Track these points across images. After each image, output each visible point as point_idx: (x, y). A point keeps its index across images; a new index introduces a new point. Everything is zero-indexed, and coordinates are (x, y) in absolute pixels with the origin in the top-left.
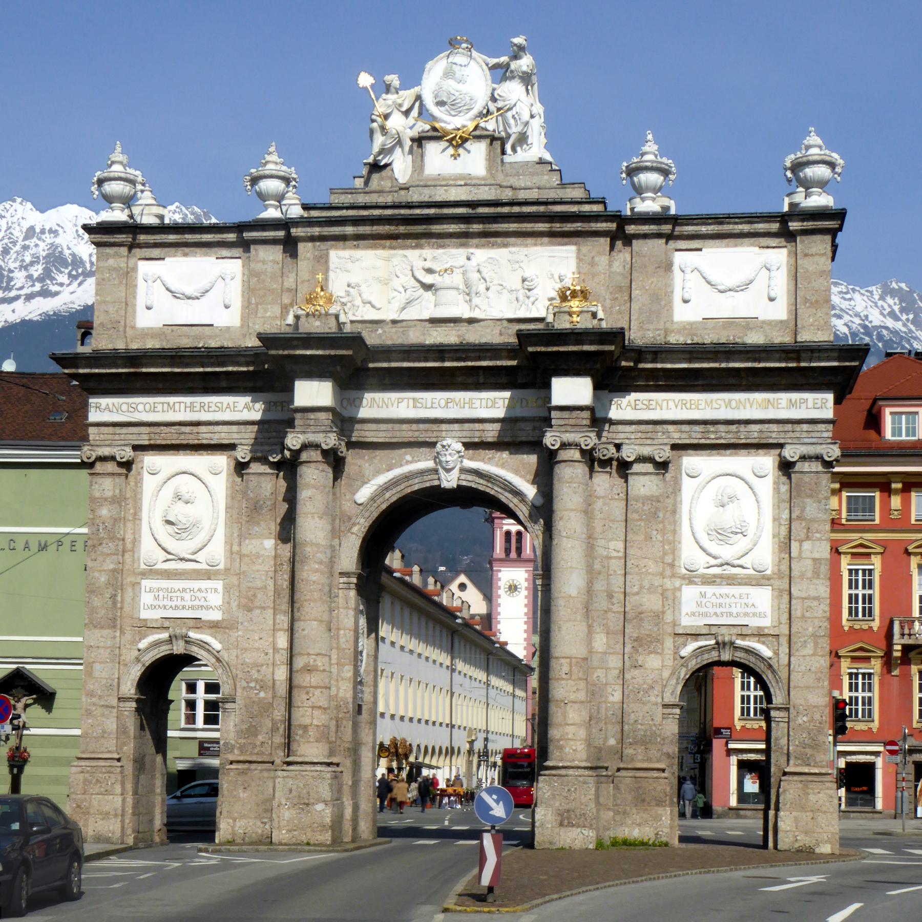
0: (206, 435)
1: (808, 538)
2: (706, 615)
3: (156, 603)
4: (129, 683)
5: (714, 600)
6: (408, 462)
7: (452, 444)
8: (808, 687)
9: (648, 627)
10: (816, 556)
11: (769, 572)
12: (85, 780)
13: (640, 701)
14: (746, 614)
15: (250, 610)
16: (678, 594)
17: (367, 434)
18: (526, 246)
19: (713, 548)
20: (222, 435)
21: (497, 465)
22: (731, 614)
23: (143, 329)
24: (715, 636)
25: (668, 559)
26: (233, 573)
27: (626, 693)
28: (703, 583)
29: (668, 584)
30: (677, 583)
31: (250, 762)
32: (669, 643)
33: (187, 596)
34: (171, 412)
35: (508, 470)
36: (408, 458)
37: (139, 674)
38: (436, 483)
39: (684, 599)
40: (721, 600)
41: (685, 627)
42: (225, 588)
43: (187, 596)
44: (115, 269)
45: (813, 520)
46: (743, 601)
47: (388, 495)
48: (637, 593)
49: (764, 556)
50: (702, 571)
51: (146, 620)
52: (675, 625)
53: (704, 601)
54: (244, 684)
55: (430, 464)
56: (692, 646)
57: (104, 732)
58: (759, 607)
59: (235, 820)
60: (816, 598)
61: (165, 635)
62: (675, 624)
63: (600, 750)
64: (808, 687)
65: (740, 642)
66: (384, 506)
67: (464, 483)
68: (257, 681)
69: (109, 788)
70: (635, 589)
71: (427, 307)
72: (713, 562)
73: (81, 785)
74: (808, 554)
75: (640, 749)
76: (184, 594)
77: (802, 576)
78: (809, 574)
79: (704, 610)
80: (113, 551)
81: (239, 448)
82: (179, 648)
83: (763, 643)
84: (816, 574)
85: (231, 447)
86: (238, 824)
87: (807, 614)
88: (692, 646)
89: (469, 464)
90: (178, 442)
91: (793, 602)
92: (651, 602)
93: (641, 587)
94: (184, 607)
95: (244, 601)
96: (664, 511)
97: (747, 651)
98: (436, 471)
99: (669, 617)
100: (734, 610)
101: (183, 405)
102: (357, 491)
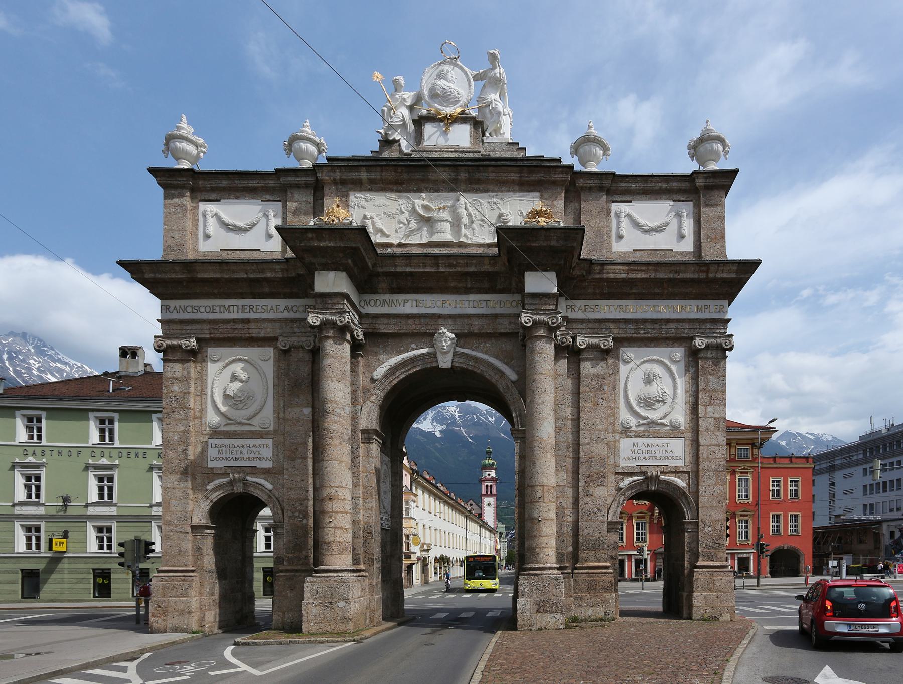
0: (254, 332)
1: (711, 403)
2: (638, 459)
3: (219, 456)
4: (200, 515)
5: (643, 448)
6: (413, 349)
7: (447, 336)
8: (711, 507)
9: (596, 468)
10: (717, 416)
11: (682, 428)
12: (164, 587)
13: (591, 520)
14: (666, 458)
15: (294, 460)
16: (617, 445)
17: (381, 327)
18: (502, 192)
19: (642, 412)
20: (268, 331)
21: (482, 352)
22: (656, 458)
23: (204, 252)
24: (644, 474)
25: (611, 419)
26: (280, 434)
27: (581, 514)
28: (636, 436)
29: (610, 437)
30: (617, 437)
31: (297, 571)
32: (611, 479)
33: (245, 451)
34: (226, 313)
35: (490, 355)
36: (414, 346)
37: (208, 508)
38: (435, 364)
39: (621, 448)
40: (648, 448)
41: (622, 468)
42: (274, 444)
43: (245, 451)
44: (179, 205)
45: (715, 391)
46: (664, 449)
47: (398, 373)
48: (589, 444)
49: (680, 417)
50: (634, 428)
51: (212, 469)
52: (615, 466)
53: (636, 449)
54: (290, 514)
55: (432, 350)
56: (628, 481)
57: (180, 551)
58: (675, 453)
59: (284, 613)
60: (716, 445)
61: (226, 480)
62: (616, 466)
63: (563, 554)
64: (711, 507)
65: (662, 477)
66: (395, 382)
67: (457, 364)
68: (300, 512)
69: (183, 592)
70: (587, 441)
71: (424, 237)
72: (642, 422)
73: (161, 590)
74: (712, 415)
75: (591, 553)
76: (242, 449)
77: (707, 430)
78: (712, 429)
79: (637, 455)
80: (183, 417)
81: (281, 339)
82: (239, 489)
83: (679, 478)
84: (717, 428)
85: (276, 339)
86: (287, 616)
87: (711, 456)
88: (628, 481)
89: (459, 349)
90: (233, 336)
91: (701, 448)
92: (599, 450)
93: (591, 439)
94: (242, 459)
95: (288, 453)
96: (607, 385)
97: (668, 484)
98: (434, 355)
99: (611, 461)
100: (658, 455)
101: (236, 308)
102: (374, 370)
